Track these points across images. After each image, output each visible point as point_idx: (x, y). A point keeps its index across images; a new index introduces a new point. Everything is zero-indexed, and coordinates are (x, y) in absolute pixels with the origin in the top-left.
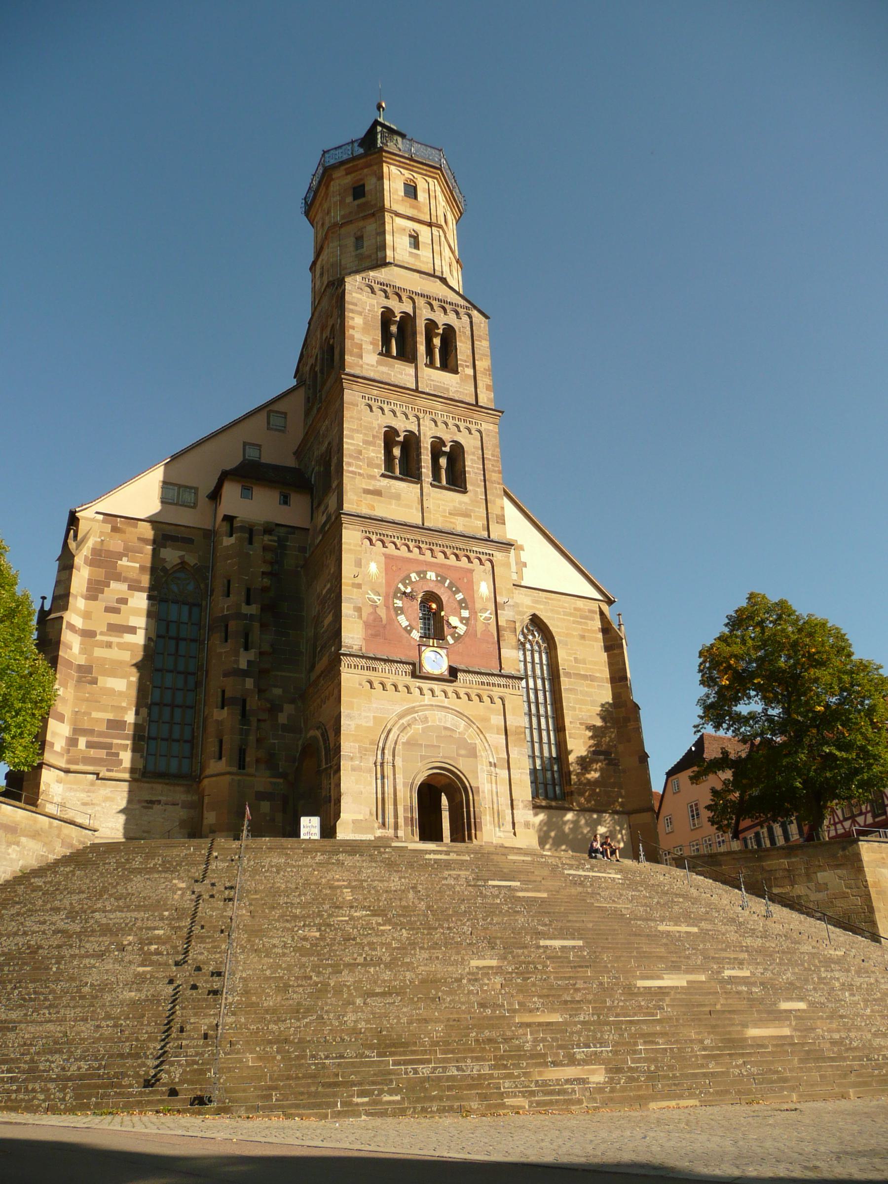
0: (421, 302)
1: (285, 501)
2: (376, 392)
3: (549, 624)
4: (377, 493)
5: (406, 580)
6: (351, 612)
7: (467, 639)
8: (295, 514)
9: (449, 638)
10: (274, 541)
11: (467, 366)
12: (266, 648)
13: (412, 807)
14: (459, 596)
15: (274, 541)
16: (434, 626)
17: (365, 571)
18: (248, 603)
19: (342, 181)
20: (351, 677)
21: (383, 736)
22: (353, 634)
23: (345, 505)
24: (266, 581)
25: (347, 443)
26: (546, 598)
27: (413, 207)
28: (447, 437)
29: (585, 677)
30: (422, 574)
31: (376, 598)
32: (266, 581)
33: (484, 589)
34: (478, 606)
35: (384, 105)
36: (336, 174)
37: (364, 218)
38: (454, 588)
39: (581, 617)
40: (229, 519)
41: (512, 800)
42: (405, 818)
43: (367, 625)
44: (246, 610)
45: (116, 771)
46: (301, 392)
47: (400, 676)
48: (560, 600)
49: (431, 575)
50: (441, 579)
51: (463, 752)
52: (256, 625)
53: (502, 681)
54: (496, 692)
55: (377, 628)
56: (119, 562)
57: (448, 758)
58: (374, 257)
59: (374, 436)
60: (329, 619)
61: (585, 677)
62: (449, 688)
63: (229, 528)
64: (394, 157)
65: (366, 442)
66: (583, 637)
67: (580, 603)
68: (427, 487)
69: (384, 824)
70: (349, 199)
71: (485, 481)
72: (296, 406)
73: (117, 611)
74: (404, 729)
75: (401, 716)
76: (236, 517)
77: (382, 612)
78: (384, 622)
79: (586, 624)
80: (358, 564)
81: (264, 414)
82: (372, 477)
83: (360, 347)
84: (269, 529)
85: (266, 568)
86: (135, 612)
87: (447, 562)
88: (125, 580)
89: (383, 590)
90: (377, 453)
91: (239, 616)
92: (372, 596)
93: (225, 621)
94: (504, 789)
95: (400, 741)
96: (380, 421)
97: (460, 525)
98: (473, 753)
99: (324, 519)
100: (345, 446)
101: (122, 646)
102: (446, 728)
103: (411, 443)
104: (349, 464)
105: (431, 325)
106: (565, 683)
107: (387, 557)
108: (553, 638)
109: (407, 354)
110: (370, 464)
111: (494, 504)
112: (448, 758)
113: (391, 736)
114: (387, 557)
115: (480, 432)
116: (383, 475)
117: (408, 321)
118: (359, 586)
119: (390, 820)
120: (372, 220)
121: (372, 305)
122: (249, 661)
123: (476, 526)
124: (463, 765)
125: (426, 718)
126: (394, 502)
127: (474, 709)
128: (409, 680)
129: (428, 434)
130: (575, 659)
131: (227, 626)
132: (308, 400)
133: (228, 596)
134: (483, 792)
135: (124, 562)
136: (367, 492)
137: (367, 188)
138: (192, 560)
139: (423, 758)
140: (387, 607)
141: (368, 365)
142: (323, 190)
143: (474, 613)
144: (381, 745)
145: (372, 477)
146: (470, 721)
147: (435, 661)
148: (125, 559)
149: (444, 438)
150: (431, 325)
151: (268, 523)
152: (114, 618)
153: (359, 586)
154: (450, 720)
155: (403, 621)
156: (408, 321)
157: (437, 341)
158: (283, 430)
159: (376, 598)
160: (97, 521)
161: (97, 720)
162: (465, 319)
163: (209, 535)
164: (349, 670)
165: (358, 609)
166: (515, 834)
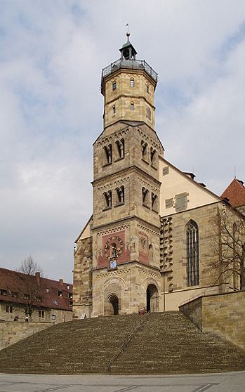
50: (116, 237)
54: (128, 268)
67: (209, 207)
80: (96, 243)
98: (120, 288)
136: (99, 218)
155: (106, 255)
165: (96, 256)
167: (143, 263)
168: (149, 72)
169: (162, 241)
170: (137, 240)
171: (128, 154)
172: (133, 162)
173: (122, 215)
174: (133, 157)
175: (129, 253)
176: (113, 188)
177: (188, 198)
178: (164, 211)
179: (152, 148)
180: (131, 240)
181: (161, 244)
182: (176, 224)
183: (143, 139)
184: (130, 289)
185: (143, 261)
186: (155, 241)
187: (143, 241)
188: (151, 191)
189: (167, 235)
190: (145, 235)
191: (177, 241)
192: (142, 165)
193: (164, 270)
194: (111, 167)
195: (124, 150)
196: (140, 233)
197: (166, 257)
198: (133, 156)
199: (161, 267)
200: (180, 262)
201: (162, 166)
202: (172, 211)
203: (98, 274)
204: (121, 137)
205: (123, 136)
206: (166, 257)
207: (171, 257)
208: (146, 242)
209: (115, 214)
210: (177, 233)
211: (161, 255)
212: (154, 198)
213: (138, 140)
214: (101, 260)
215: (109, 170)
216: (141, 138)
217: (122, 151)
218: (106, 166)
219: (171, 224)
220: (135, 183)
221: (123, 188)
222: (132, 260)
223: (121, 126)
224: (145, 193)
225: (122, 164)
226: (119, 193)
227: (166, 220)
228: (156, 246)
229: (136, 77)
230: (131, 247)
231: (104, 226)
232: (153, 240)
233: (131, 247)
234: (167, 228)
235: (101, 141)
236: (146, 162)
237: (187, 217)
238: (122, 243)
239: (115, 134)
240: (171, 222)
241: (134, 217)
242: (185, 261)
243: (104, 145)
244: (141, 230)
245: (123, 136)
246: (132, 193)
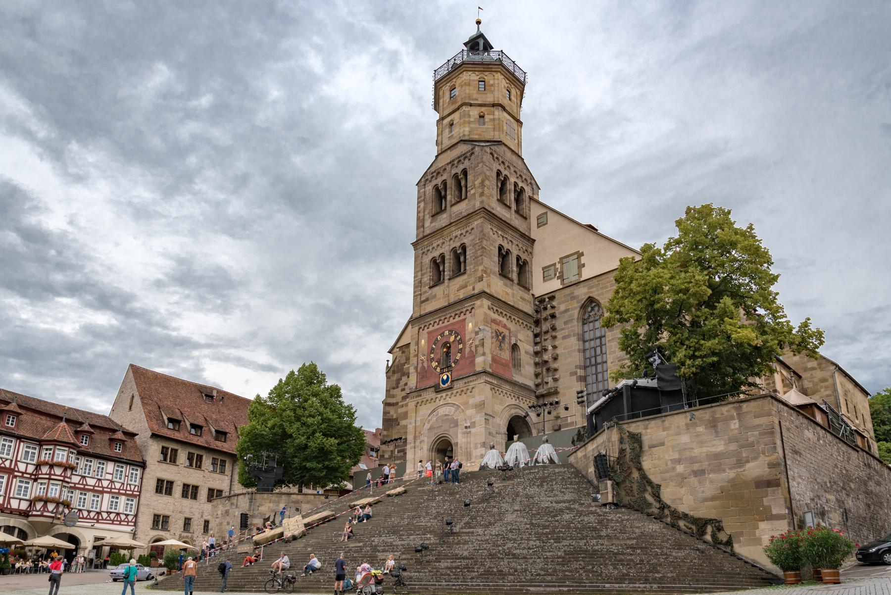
4: (427, 300)
7: (461, 362)
30: (442, 335)
34: (467, 338)
47: (430, 395)
50: (451, 332)
53: (474, 378)
62: (449, 393)
65: (422, 275)
77: (425, 365)
82: (425, 292)
89: (426, 353)
98: (456, 424)
107: (429, 333)
114: (429, 333)
123: (469, 291)
128: (433, 395)
143: (464, 345)
145: (425, 292)
155: (434, 364)
165: (416, 368)
167: (498, 377)
168: (511, 68)
169: (538, 339)
170: (487, 334)
171: (472, 192)
172: (482, 202)
173: (462, 291)
174: (482, 194)
175: (473, 357)
176: (446, 249)
177: (583, 260)
178: (540, 287)
179: (516, 184)
180: (477, 333)
181: (536, 344)
182: (562, 307)
183: (499, 168)
184: (473, 424)
185: (501, 372)
186: (524, 338)
187: (500, 337)
188: (515, 252)
189: (545, 326)
190: (505, 326)
191: (564, 338)
192: (499, 209)
193: (542, 391)
194: (444, 215)
195: (466, 187)
196: (494, 321)
197: (544, 367)
198: (483, 193)
199: (537, 386)
200: (572, 374)
201: (535, 212)
202: (556, 284)
203: (419, 399)
204: (461, 167)
205: (467, 164)
206: (544, 367)
207: (555, 366)
208: (507, 340)
209: (453, 289)
210: (565, 323)
211: (536, 364)
212: (523, 266)
213: (491, 169)
214: (423, 374)
215: (443, 220)
216: (496, 166)
217: (464, 189)
218: (437, 214)
219: (553, 307)
220: (483, 236)
221: (464, 247)
222: (478, 369)
223: (463, 148)
224: (504, 255)
225: (463, 208)
226: (457, 257)
227: (543, 302)
228: (526, 347)
229: (488, 77)
230: (476, 346)
231: (431, 313)
232: (520, 336)
233: (476, 346)
234: (545, 314)
235: (429, 177)
236: (506, 205)
237: (582, 292)
238: (461, 341)
239: (451, 163)
240: (554, 303)
241: (483, 294)
242: (581, 372)
243: (434, 183)
244: (496, 316)
246: (479, 253)
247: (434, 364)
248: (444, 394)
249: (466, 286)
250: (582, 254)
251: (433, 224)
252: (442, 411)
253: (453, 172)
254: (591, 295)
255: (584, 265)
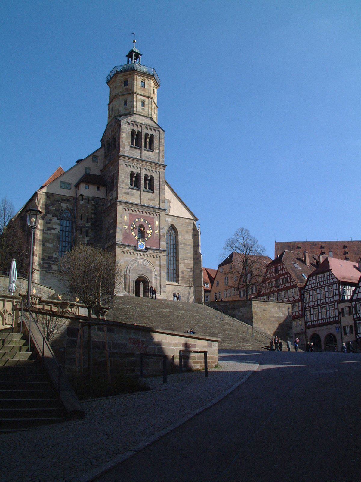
0: (144, 127)
1: (98, 189)
2: (129, 160)
3: (176, 227)
4: (128, 194)
5: (135, 222)
6: (119, 231)
8: (101, 194)
9: (146, 239)
10: (95, 203)
11: (157, 149)
12: (92, 237)
13: (133, 286)
14: (150, 226)
15: (95, 203)
16: (142, 234)
17: (123, 217)
18: (87, 222)
19: (120, 78)
20: (118, 250)
21: (126, 267)
22: (119, 238)
23: (118, 198)
24: (93, 216)
25: (120, 178)
26: (176, 219)
27: (143, 91)
28: (149, 175)
29: (186, 245)
30: (139, 219)
31: (126, 227)
32: (93, 216)
33: (157, 223)
34: (155, 229)
35: (135, 41)
36: (119, 76)
37: (128, 94)
38: (149, 223)
39: (187, 225)
40: (82, 196)
41: (160, 285)
42: (132, 289)
43: (123, 235)
44: (87, 225)
45: (51, 271)
46: (103, 148)
47: (132, 250)
48: (180, 219)
49: (142, 220)
50: (145, 220)
51: (148, 272)
52: (90, 229)
54: (158, 254)
55: (126, 236)
56: (49, 208)
57: (144, 273)
58: (130, 110)
59: (127, 175)
60: (112, 231)
61: (186, 245)
63: (81, 198)
64: (139, 72)
65: (125, 177)
66: (187, 232)
67: (187, 221)
68: (142, 191)
69: (126, 291)
70: (123, 85)
71: (160, 189)
72: (101, 154)
73: (49, 223)
74: (132, 265)
75: (132, 261)
76: (84, 195)
77: (128, 231)
78: (128, 234)
79: (188, 227)
80: (122, 216)
81: (91, 157)
83: (125, 145)
84: (94, 199)
85: (93, 211)
86: (55, 223)
87: (147, 215)
88: (51, 213)
89: (128, 224)
90: (128, 181)
91: (85, 226)
92: (125, 226)
93: (81, 227)
94: (158, 282)
95: (131, 268)
96: (129, 170)
97: (151, 204)
98: (150, 272)
99: (111, 198)
100: (119, 179)
101: (51, 234)
102: (144, 265)
103: (138, 176)
104: (120, 185)
105: (146, 135)
106: (180, 246)
107: (130, 214)
108: (178, 232)
109: (139, 146)
110: (126, 184)
111: (162, 196)
112: (144, 273)
113: (129, 267)
114: (130, 214)
115: (159, 172)
116: (130, 188)
117: (139, 133)
118: (121, 223)
119: (128, 289)
120: (130, 95)
121: (129, 129)
122: (88, 241)
123: (155, 204)
124: (148, 275)
125: (138, 261)
126: (132, 196)
127: (152, 259)
129: (143, 173)
130: (184, 239)
131: (81, 229)
132: (105, 152)
133: (82, 220)
134: (153, 283)
135: (51, 208)
136: (125, 193)
137: (129, 83)
138: (70, 207)
139: (137, 273)
140: (129, 230)
141: (126, 150)
142: (114, 79)
144: (126, 269)
145: (126, 188)
146: (150, 263)
147: (142, 245)
148: (51, 207)
149: (148, 175)
150: (146, 135)
151: (93, 197)
152: (48, 226)
153: (121, 223)
154: (145, 262)
156: (139, 133)
157: (148, 140)
158: (97, 162)
159: (126, 227)
160: (43, 195)
161: (46, 256)
162: (157, 132)
163: (75, 198)
164: (118, 248)
165: (121, 230)
166: (160, 294)
245: (153, 132)
247: (133, 234)
248: (141, 253)
249: (154, 200)
250: (170, 202)
251: (131, 152)
252: (141, 262)
253: (145, 131)
254: (173, 224)
255: (171, 207)
